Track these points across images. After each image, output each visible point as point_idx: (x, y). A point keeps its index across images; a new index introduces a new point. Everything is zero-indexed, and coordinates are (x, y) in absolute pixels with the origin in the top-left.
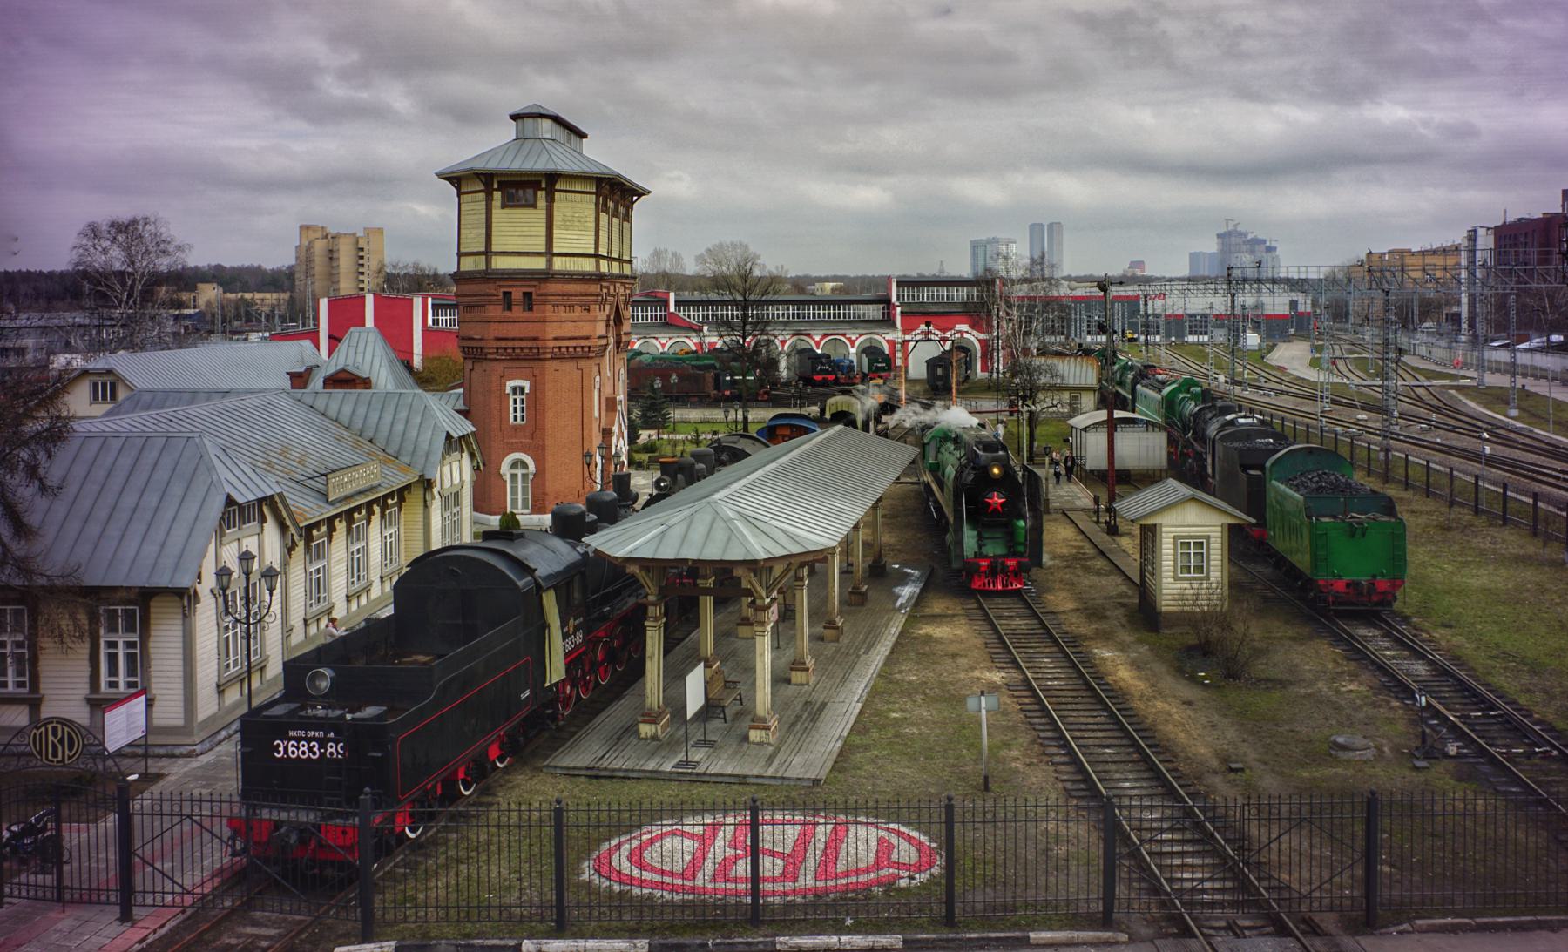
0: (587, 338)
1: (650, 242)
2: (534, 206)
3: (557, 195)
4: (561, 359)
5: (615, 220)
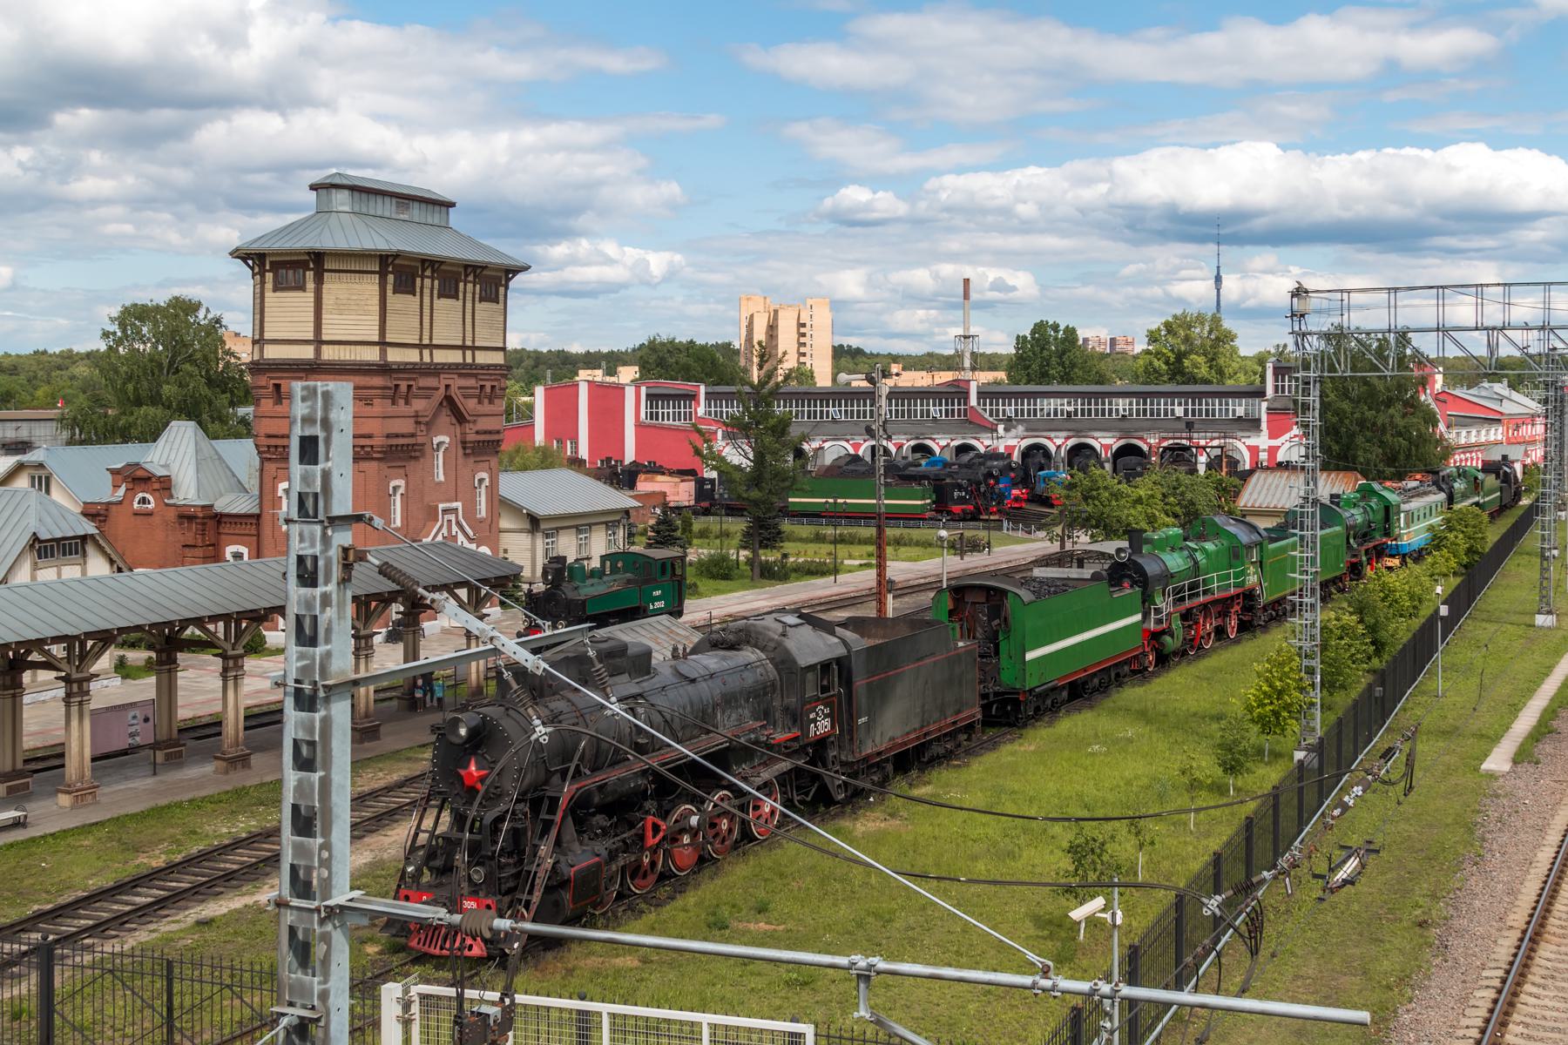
0: (370, 436)
1: (529, 325)
2: (302, 288)
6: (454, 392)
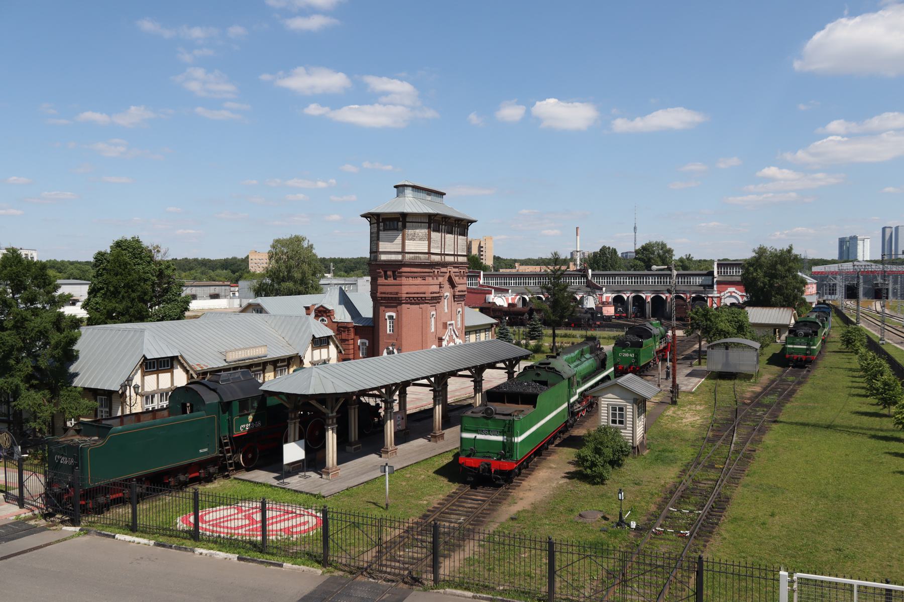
4: (411, 304)
5: (449, 236)
6: (453, 275)
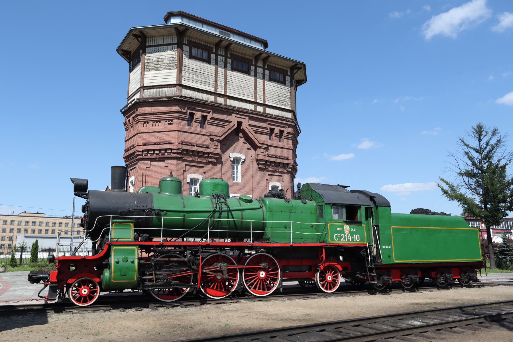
0: (170, 143)
3: (148, 49)
6: (244, 127)
